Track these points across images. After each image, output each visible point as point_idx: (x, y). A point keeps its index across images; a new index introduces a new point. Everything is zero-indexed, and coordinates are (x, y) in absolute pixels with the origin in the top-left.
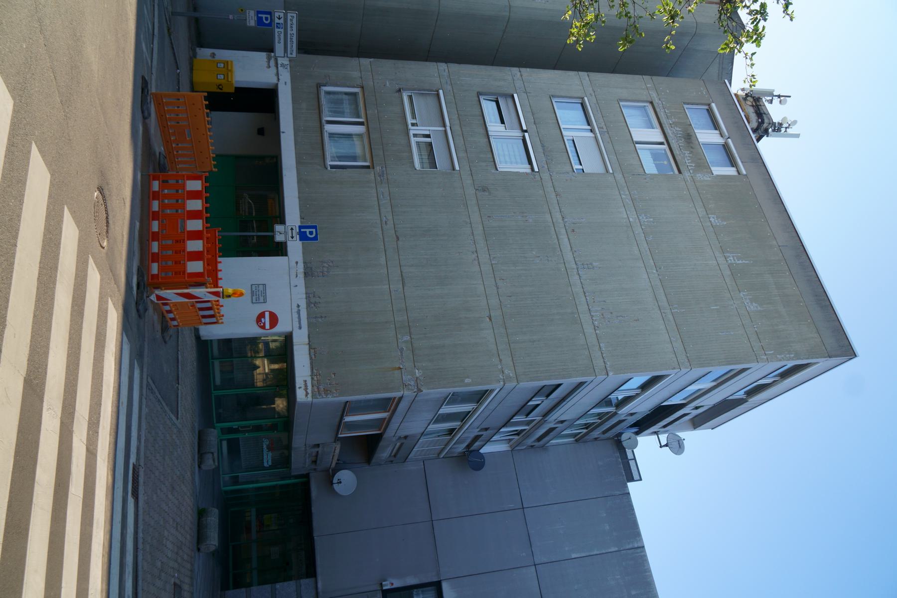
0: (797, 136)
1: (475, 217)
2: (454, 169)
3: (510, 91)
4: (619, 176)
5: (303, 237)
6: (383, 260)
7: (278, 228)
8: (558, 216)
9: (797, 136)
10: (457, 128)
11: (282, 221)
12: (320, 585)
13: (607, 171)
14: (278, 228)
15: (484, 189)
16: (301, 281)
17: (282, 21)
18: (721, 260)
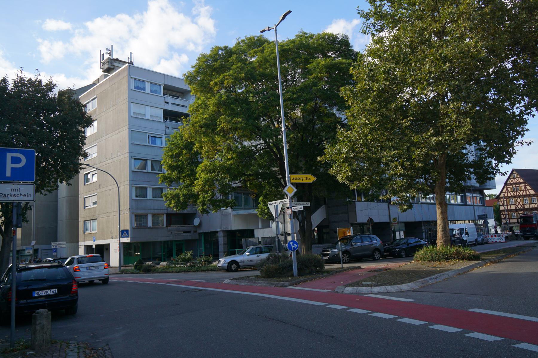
0: (112, 46)
1: (104, 189)
2: (96, 195)
3: (83, 175)
4: (97, 141)
5: (94, 241)
6: (110, 217)
7: (93, 247)
8: (104, 163)
9: (112, 46)
10: (90, 193)
11: (92, 246)
12: (219, 230)
13: (96, 145)
14: (93, 247)
15: (100, 186)
16: (113, 240)
17: (55, 246)
18: (111, 109)
